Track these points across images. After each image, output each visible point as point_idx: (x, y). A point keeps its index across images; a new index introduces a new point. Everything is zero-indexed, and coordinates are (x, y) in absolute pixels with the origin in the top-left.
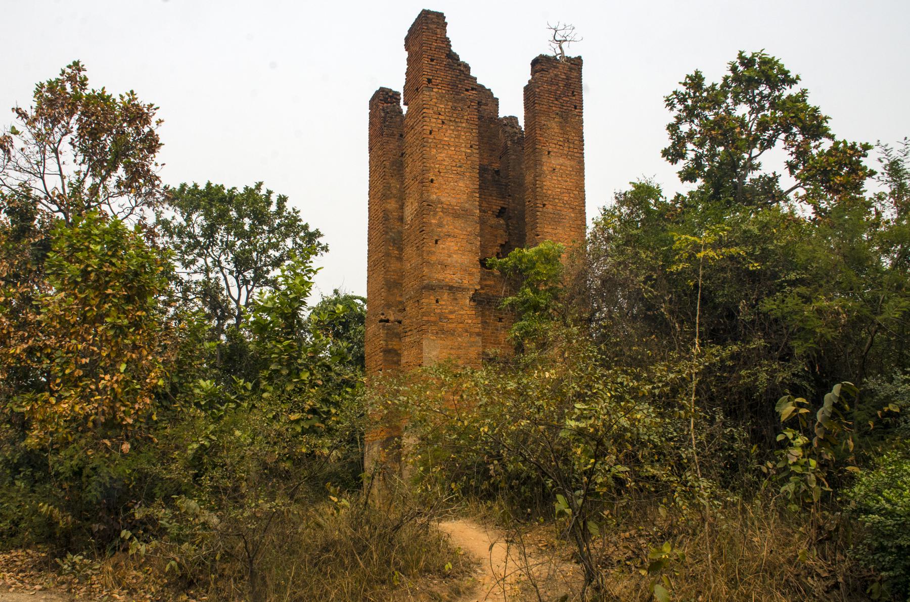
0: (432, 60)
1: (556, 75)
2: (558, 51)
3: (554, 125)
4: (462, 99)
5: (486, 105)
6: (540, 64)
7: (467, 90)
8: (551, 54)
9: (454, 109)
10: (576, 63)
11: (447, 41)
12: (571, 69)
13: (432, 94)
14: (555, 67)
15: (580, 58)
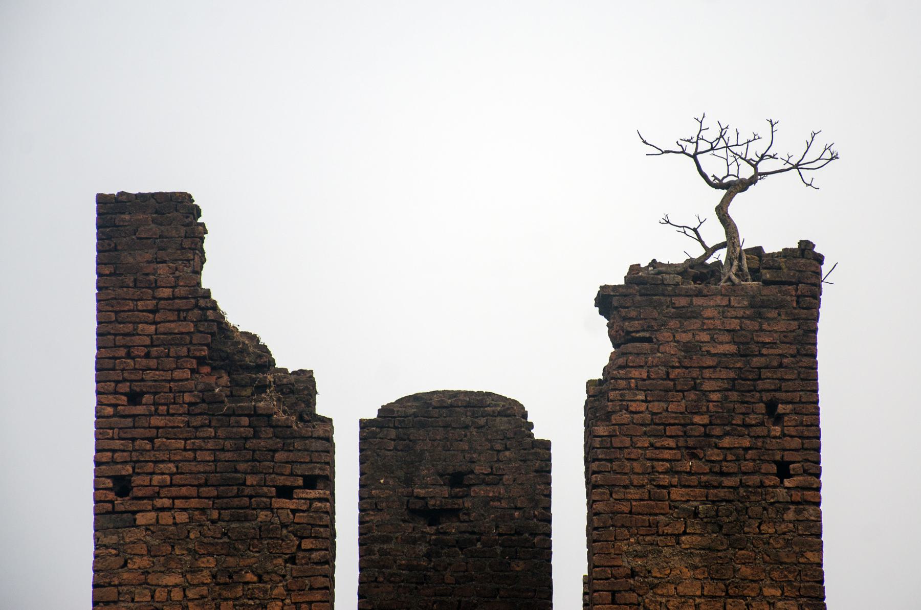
0: (134, 398)
1: (689, 349)
2: (715, 234)
3: (680, 567)
4: (265, 531)
5: (494, 478)
6: (637, 304)
7: (285, 492)
8: (677, 251)
9: (226, 579)
10: (799, 274)
11: (204, 304)
12: (758, 308)
13: (130, 535)
14: (684, 315)
15: (806, 247)
